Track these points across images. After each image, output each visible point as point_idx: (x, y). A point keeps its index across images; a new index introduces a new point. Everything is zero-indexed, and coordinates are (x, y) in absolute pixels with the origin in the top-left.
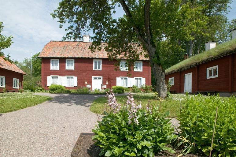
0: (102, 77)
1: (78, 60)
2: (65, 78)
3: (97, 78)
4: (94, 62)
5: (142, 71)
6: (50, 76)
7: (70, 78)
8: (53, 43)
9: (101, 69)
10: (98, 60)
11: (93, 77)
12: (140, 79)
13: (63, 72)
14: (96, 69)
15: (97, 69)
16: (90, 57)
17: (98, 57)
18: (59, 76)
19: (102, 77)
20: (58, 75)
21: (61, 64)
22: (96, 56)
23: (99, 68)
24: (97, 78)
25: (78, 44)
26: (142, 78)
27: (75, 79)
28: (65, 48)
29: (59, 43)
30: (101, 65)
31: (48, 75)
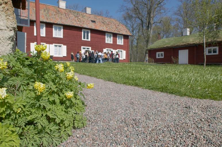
1: (66, 27)
2: (52, 46)
3: (86, 49)
4: (83, 31)
6: (34, 42)
7: (58, 46)
9: (89, 40)
10: (86, 30)
12: (121, 51)
13: (50, 40)
14: (84, 40)
15: (86, 40)
16: (80, 26)
21: (47, 28)
22: (85, 26)
23: (88, 38)
24: (86, 49)
26: (123, 50)
27: (64, 48)
30: (89, 34)
31: (31, 41)
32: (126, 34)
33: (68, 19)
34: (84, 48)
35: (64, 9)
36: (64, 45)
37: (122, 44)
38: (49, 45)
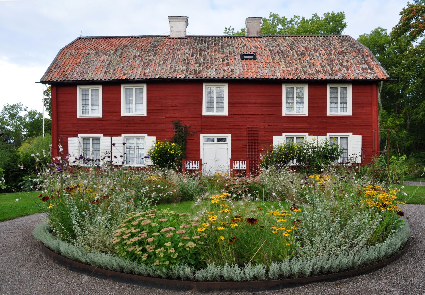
0: (228, 137)
3: (216, 140)
5: (349, 112)
8: (87, 43)
11: (202, 136)
17: (217, 77)
18: (101, 136)
19: (228, 137)
20: (101, 134)
22: (211, 73)
23: (221, 108)
25: (156, 43)
28: (119, 54)
29: (102, 42)
32: (361, 78)
33: (168, 62)
34: (208, 139)
35: (179, 38)
36: (148, 136)
37: (349, 112)
38: (110, 137)
